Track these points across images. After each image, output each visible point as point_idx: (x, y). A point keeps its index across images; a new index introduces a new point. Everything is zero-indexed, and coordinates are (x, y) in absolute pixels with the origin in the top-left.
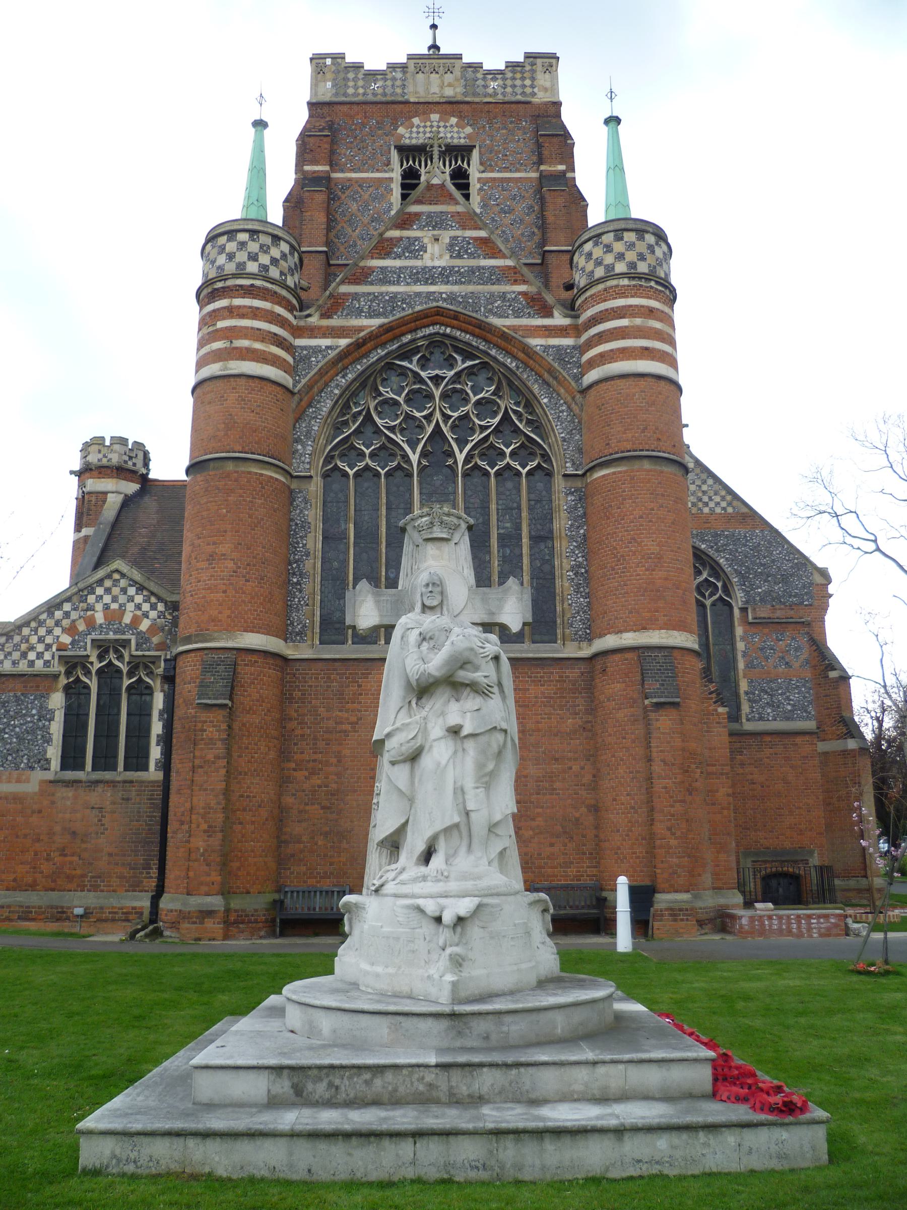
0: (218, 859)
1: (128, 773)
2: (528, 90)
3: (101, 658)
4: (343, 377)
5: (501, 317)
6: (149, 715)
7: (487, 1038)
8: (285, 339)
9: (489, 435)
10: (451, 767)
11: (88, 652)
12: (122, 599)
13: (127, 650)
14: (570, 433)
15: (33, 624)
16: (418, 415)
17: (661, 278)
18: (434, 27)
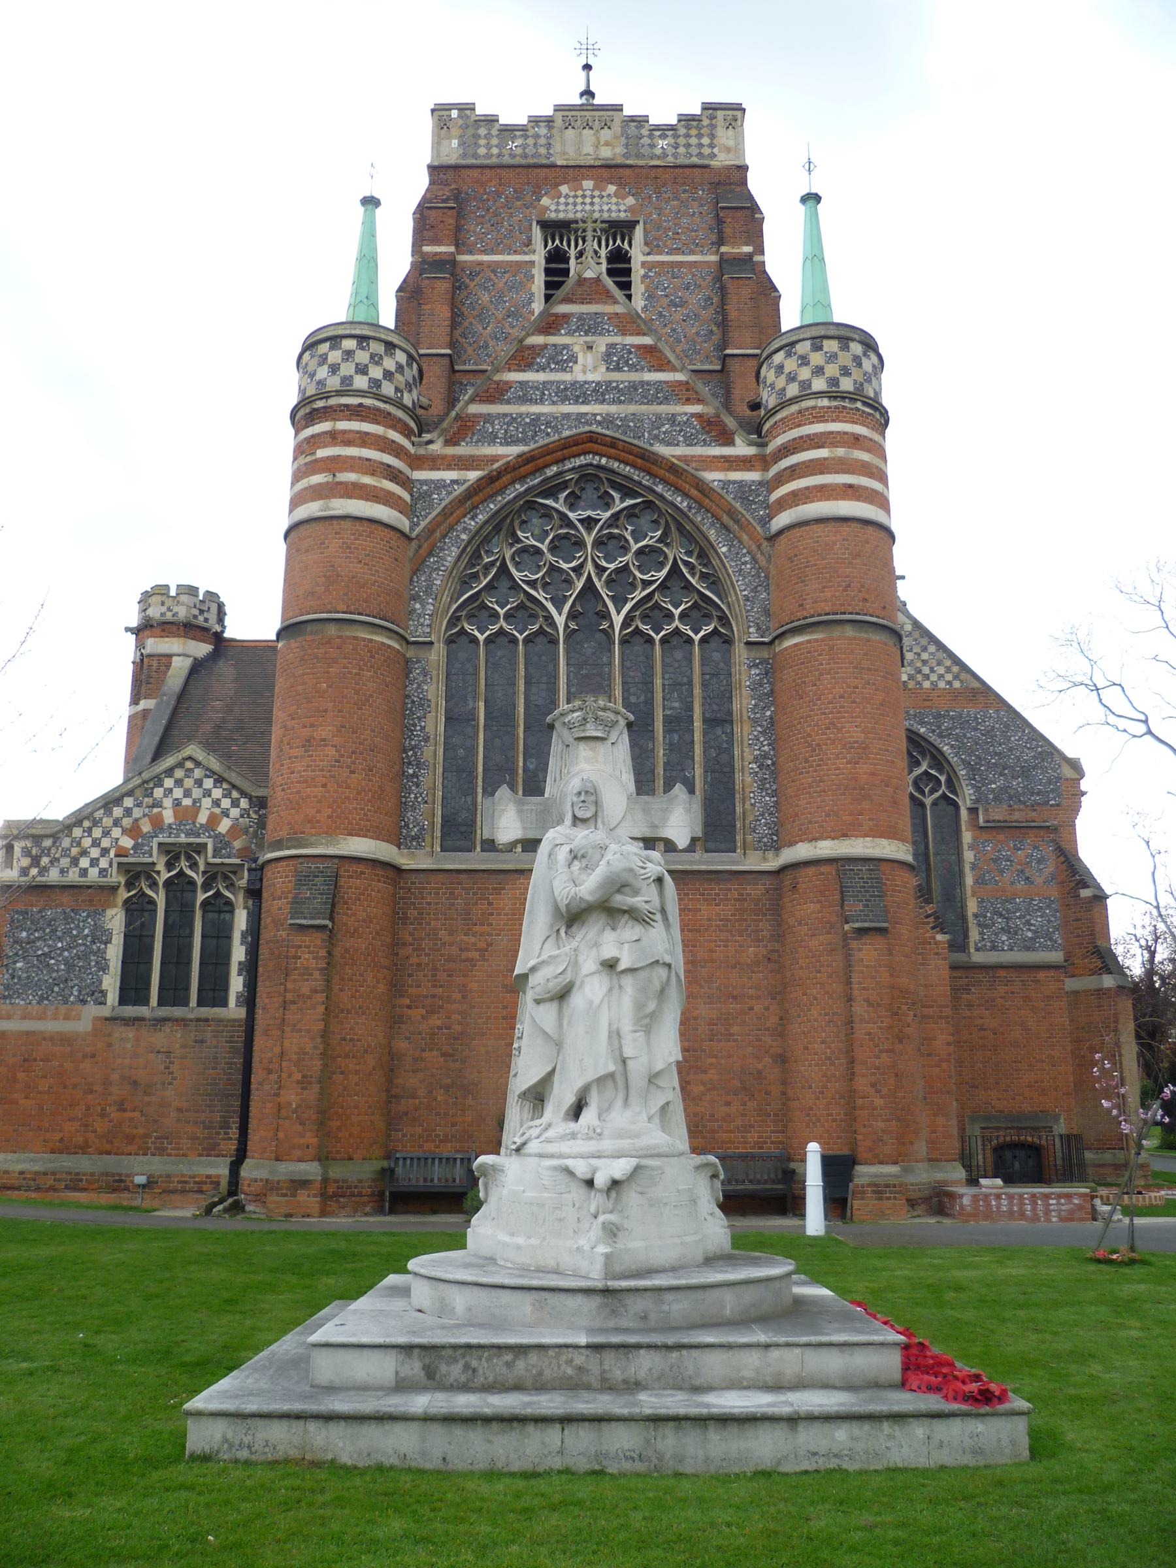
0: (314, 1117)
1: (202, 1009)
2: (706, 151)
3: (169, 866)
4: (473, 518)
5: (669, 444)
6: (229, 938)
7: (645, 1318)
8: (400, 472)
9: (653, 592)
10: (605, 1008)
12: (197, 793)
13: (203, 857)
14: (755, 590)
15: (86, 824)
16: (565, 566)
17: (870, 398)
18: (588, 67)
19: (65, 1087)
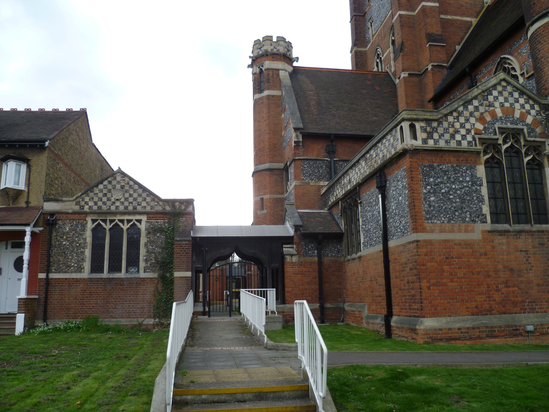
11: (496, 137)
12: (511, 100)
19: (473, 274)
